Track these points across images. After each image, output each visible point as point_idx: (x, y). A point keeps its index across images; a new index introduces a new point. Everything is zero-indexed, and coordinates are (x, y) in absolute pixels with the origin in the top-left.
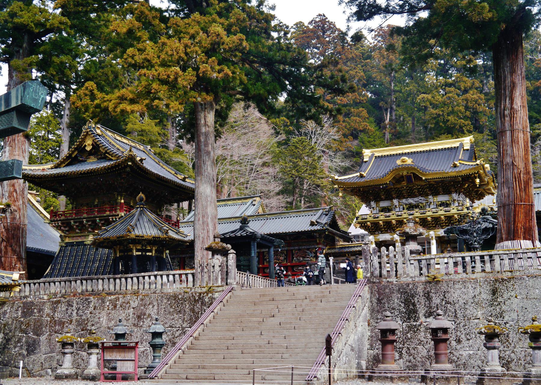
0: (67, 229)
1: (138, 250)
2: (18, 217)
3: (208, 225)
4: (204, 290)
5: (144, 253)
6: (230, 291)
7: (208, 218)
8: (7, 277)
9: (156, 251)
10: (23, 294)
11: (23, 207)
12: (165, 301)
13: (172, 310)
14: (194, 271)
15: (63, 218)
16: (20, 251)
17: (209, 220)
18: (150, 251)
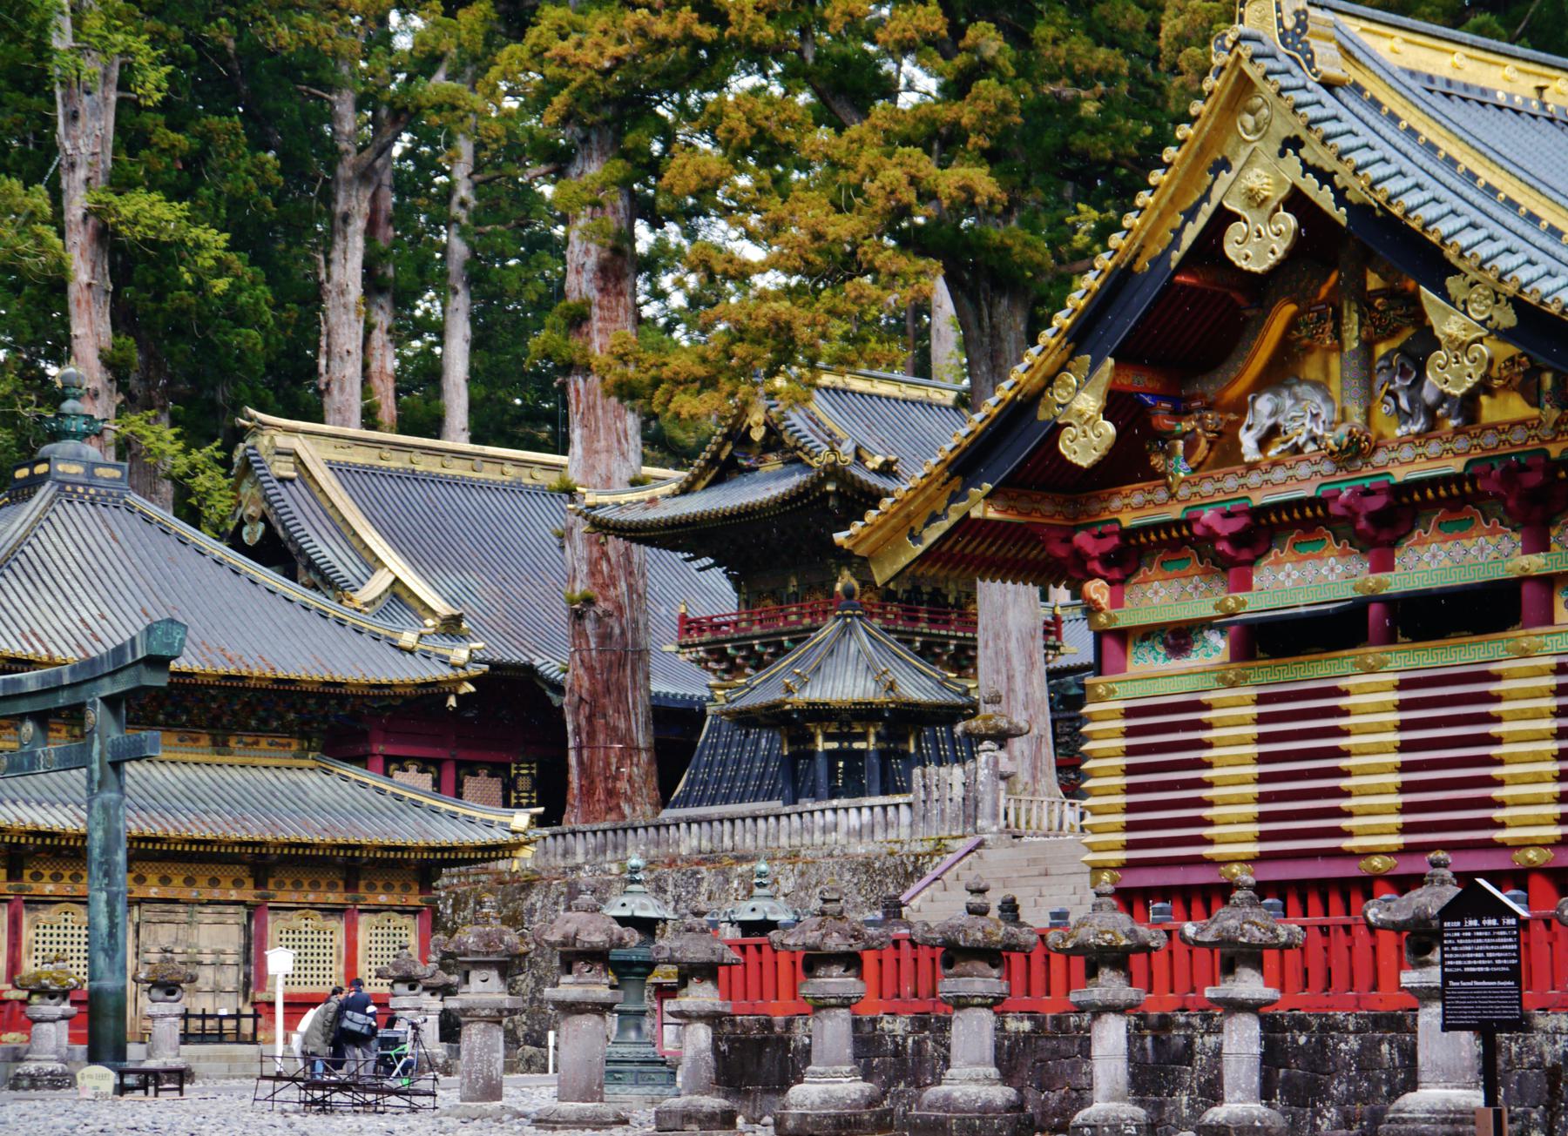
0: (723, 666)
1: (828, 737)
2: (617, 631)
3: (1008, 660)
4: (928, 846)
5: (846, 744)
6: (970, 851)
7: (1007, 640)
8: (501, 824)
9: (879, 737)
10: (570, 862)
11: (631, 598)
12: (847, 876)
13: (860, 899)
14: (910, 798)
15: (707, 636)
16: (629, 729)
17: (1013, 645)
18: (863, 737)
